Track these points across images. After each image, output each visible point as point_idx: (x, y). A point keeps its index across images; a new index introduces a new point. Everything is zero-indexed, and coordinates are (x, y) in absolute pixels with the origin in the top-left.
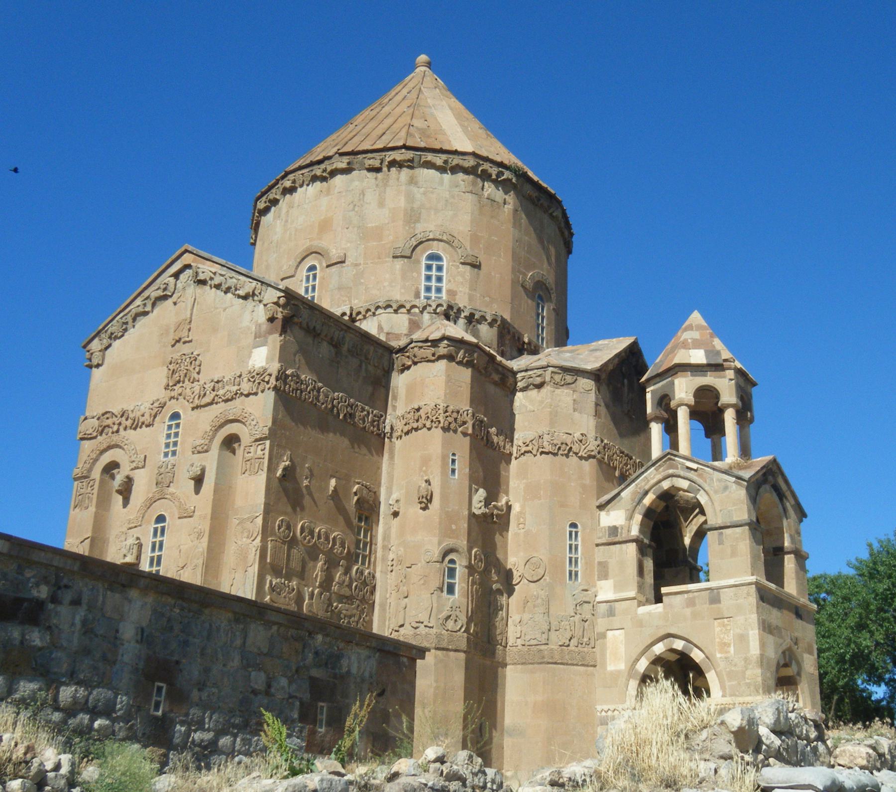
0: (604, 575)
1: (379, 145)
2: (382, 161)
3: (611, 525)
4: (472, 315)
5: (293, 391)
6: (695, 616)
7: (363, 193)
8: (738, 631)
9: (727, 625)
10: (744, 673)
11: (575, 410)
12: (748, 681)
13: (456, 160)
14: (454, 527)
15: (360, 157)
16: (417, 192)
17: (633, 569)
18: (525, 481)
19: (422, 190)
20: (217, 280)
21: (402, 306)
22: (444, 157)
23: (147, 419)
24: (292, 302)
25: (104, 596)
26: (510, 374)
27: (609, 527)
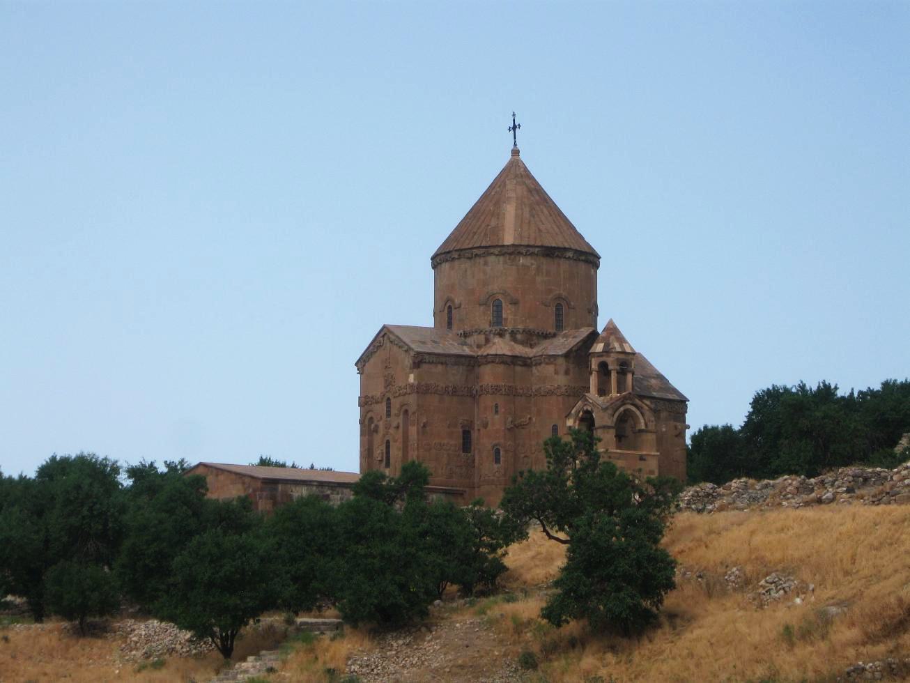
1: (470, 246)
2: (472, 254)
4: (512, 331)
13: (505, 250)
15: (464, 252)
16: (488, 269)
20: (396, 343)
21: (482, 331)
22: (499, 249)
23: (380, 400)
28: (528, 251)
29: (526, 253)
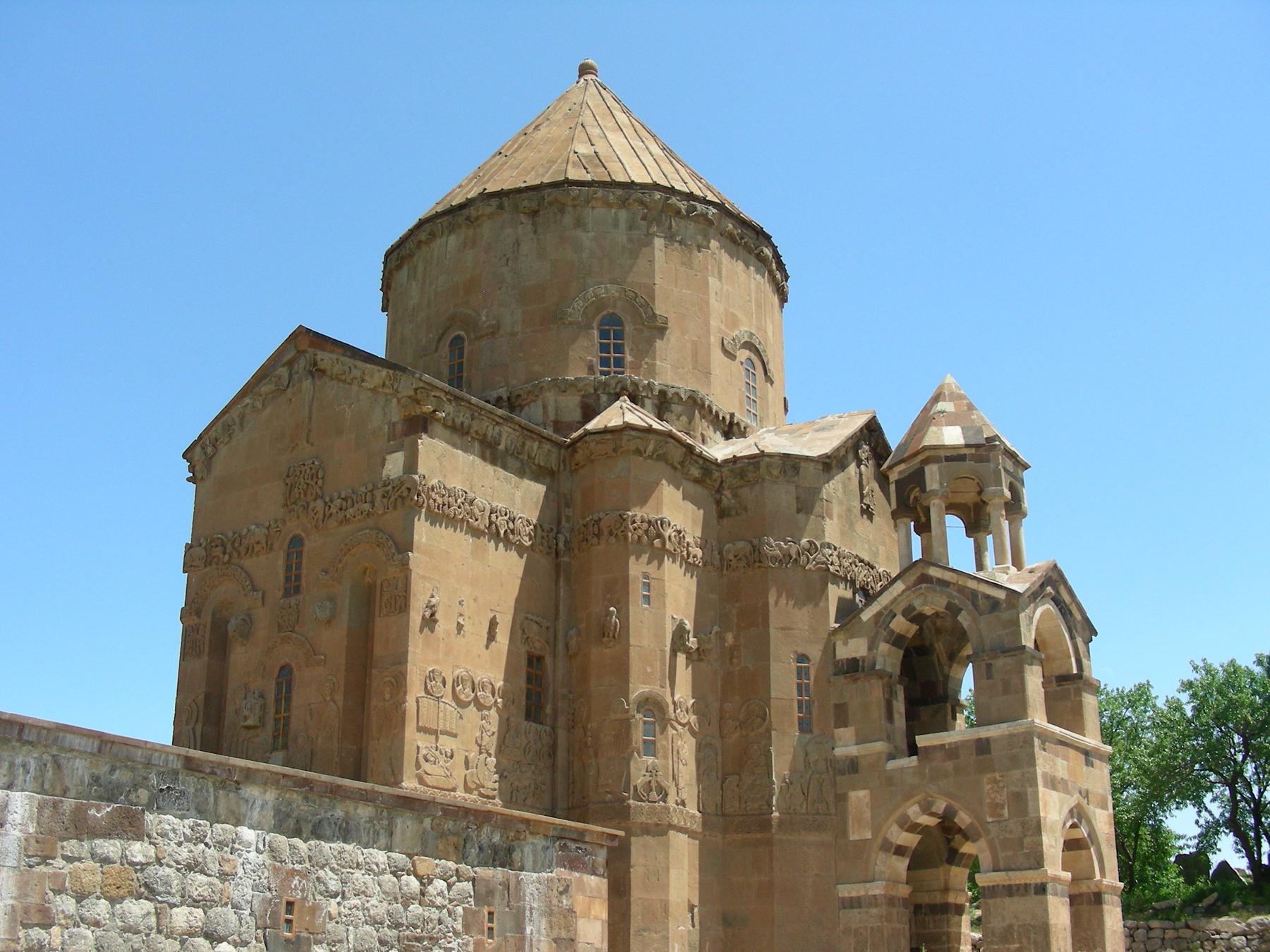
0: (842, 721)
3: (850, 657)
5: (439, 506)
6: (957, 770)
7: (517, 243)
8: (1014, 789)
9: (999, 781)
10: (1021, 841)
11: (798, 512)
12: (1026, 851)
14: (649, 670)
17: (878, 712)
18: (738, 605)
19: (591, 235)
22: (619, 192)
24: (433, 394)
25: (216, 799)
26: (714, 467)
27: (847, 659)
28: (695, 209)
29: (688, 212)
